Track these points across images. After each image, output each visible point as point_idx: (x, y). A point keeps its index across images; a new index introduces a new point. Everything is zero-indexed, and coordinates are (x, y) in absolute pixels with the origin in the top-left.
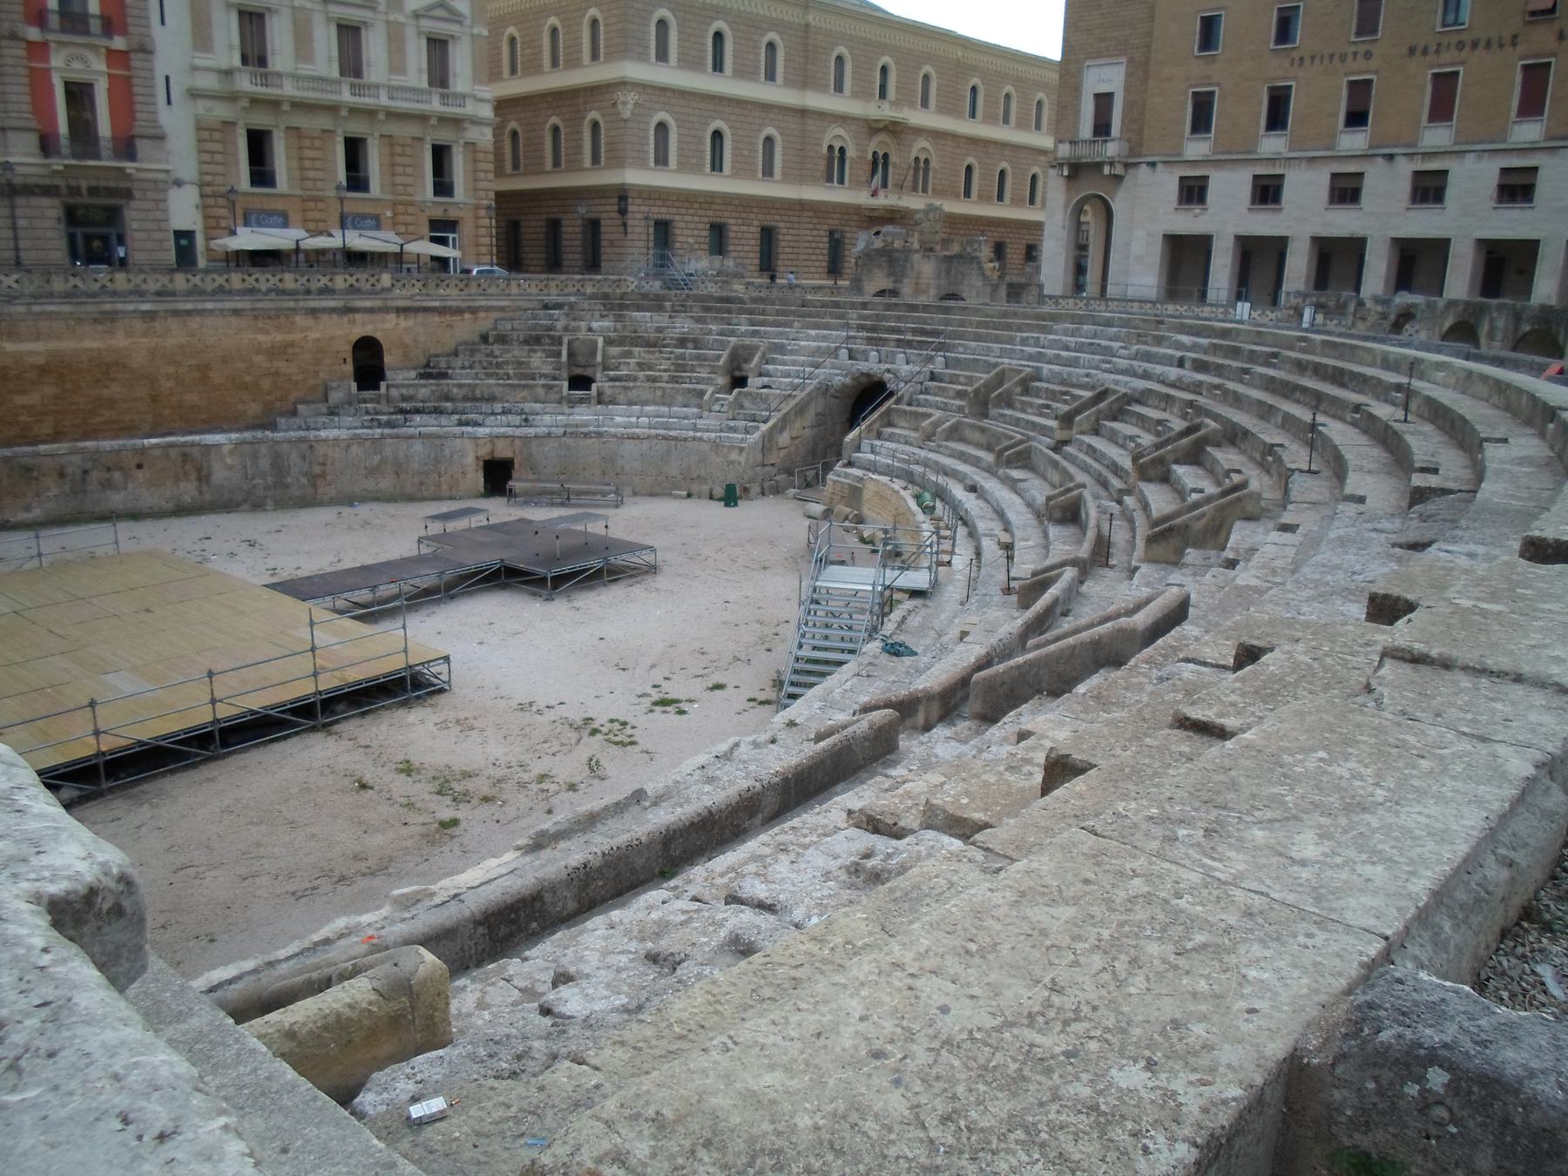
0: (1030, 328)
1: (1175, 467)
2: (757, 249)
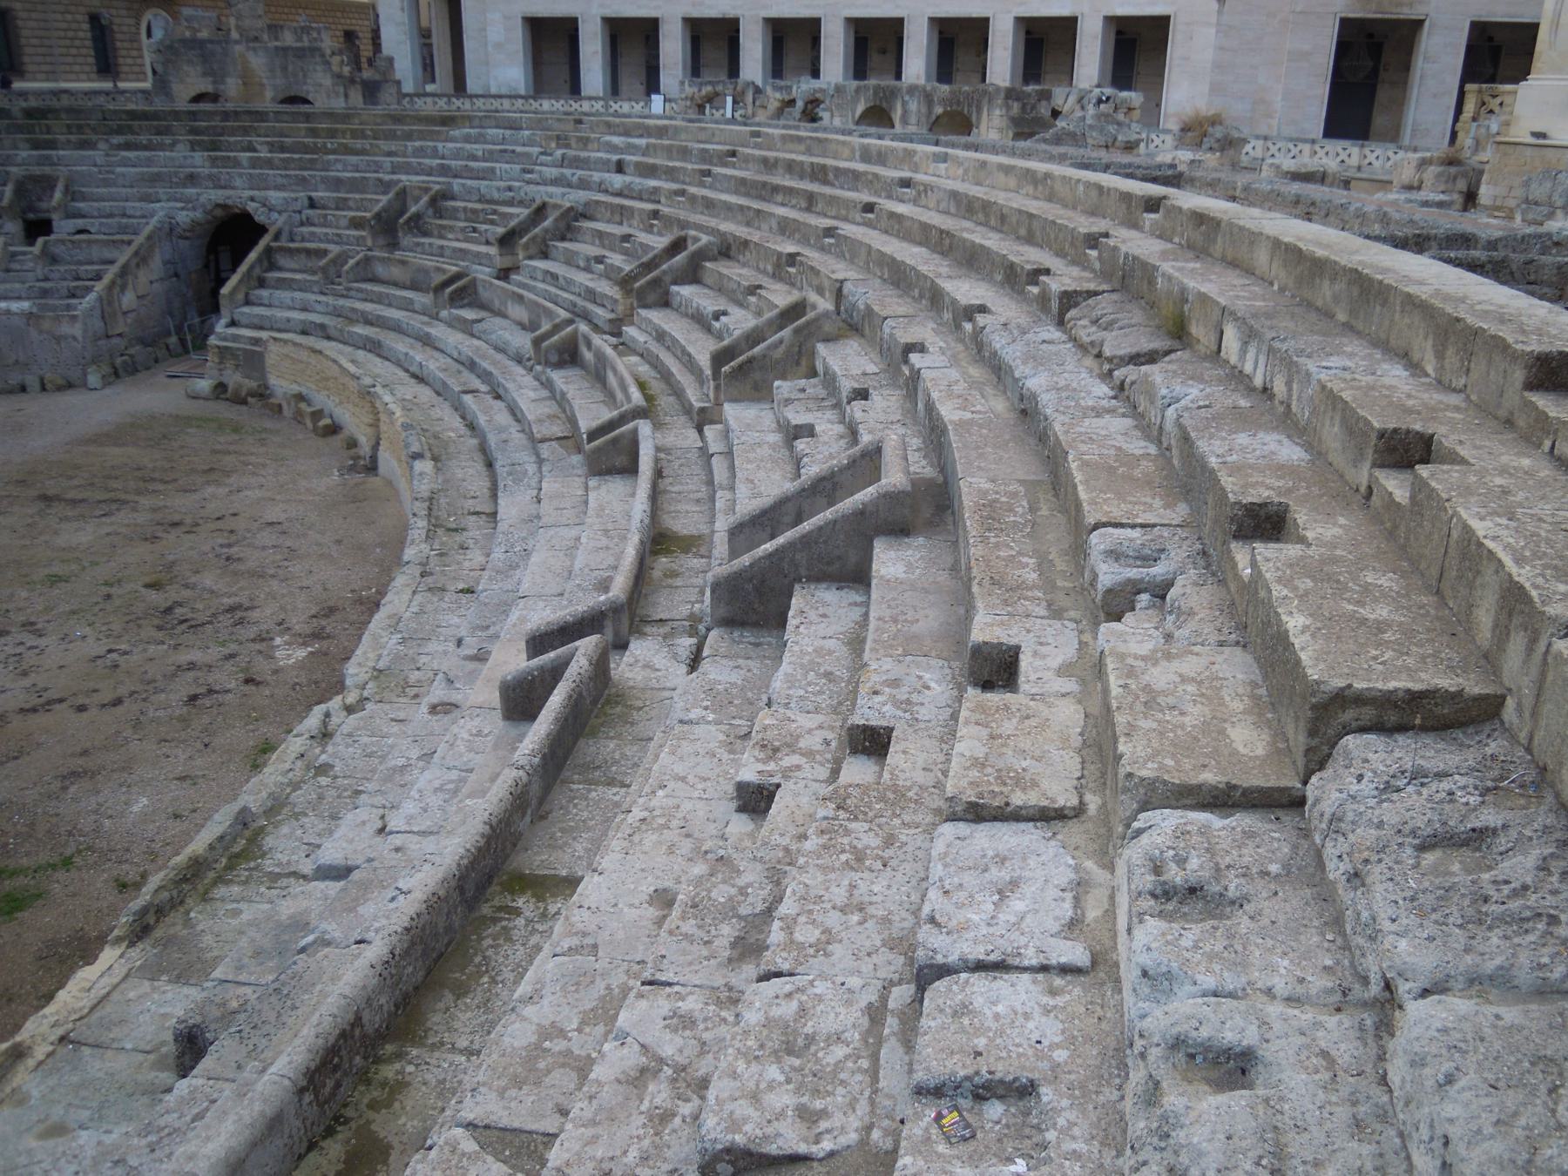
0: (422, 136)
1: (675, 288)
2: (23, 41)
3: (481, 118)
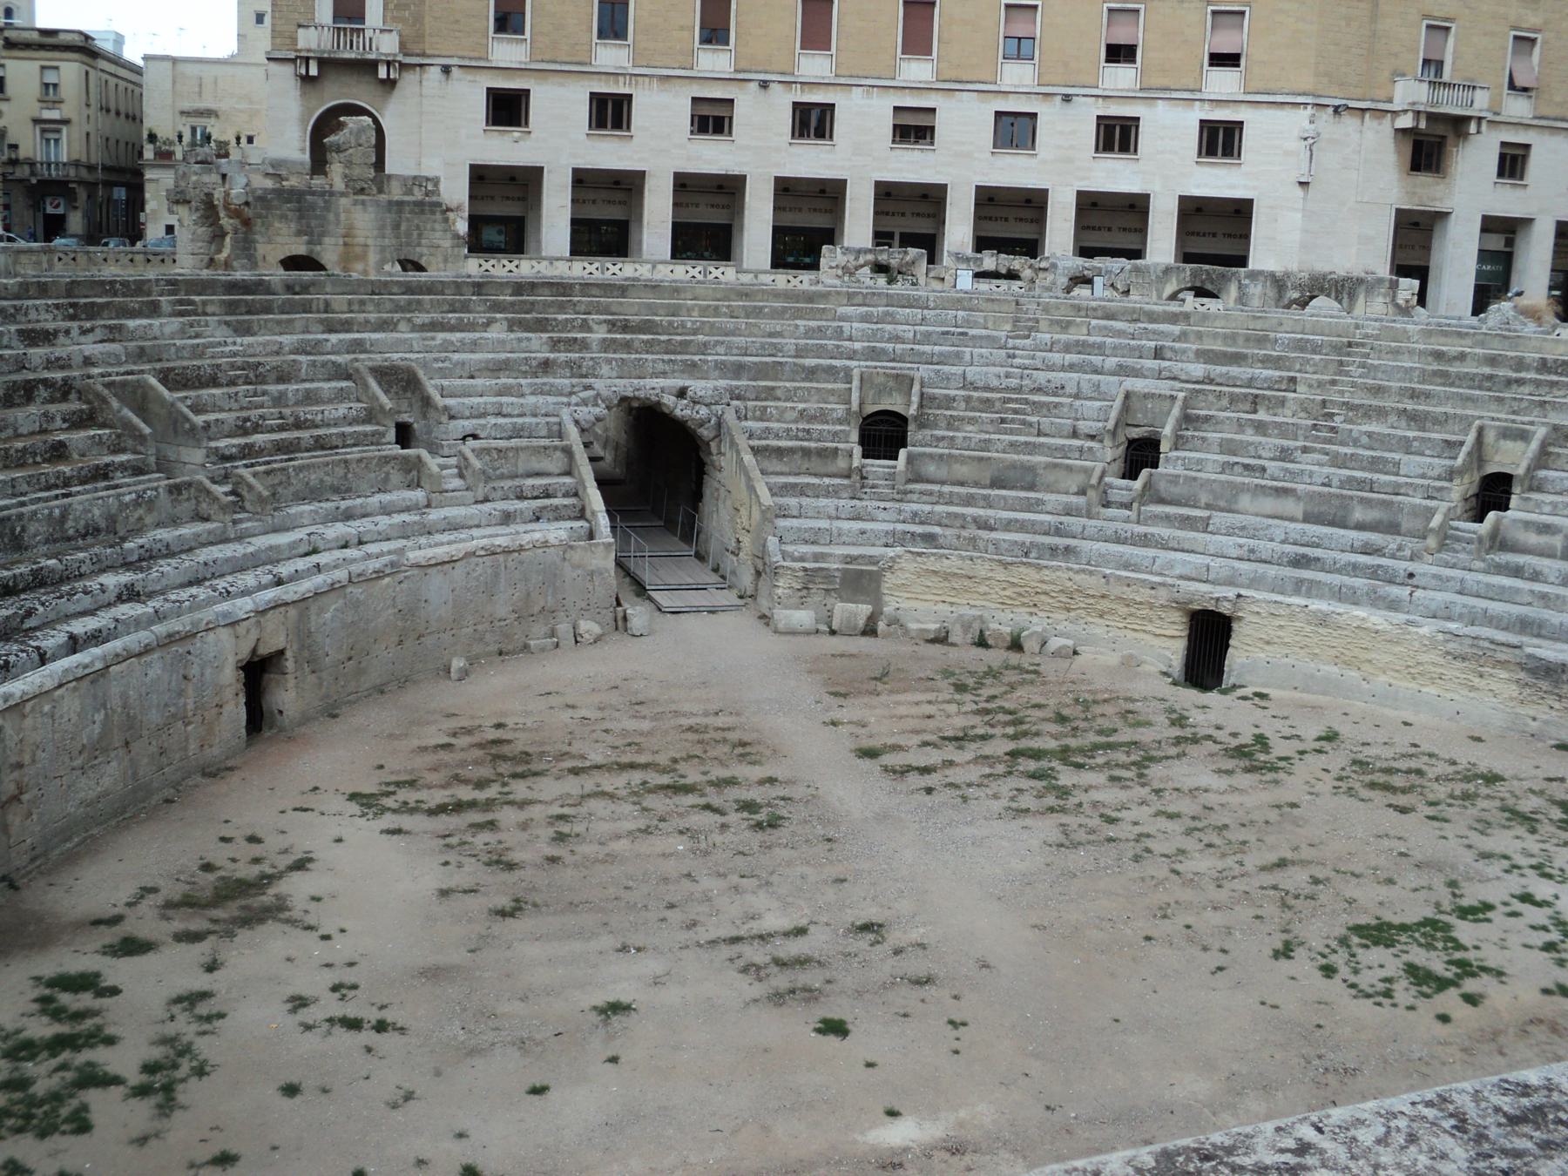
1: (1542, 473)
3: (865, 296)
